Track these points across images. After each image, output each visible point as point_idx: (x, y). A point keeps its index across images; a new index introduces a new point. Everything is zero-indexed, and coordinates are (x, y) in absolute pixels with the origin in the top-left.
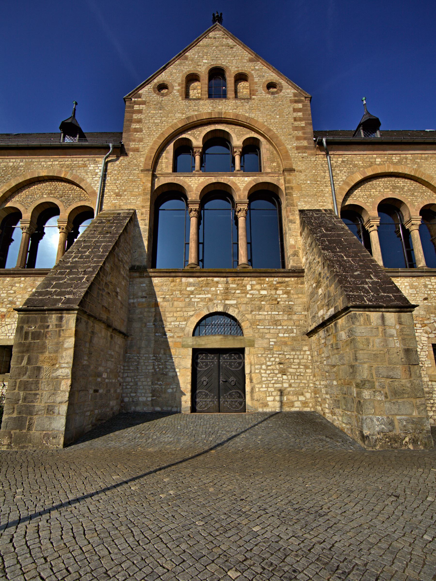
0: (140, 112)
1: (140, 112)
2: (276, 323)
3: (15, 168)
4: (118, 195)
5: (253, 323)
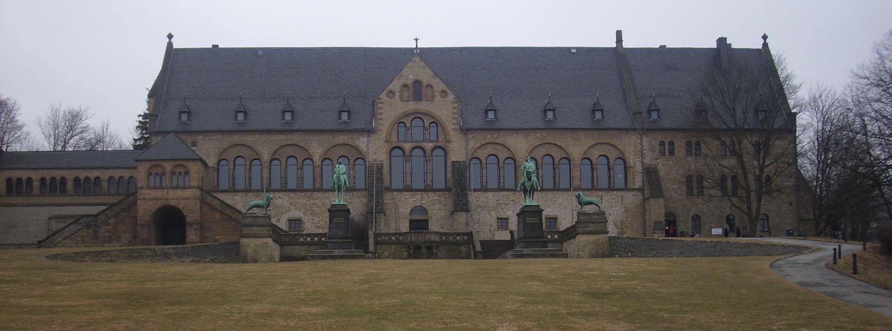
0: (381, 108)
1: (381, 108)
2: (440, 210)
4: (375, 153)
5: (432, 210)
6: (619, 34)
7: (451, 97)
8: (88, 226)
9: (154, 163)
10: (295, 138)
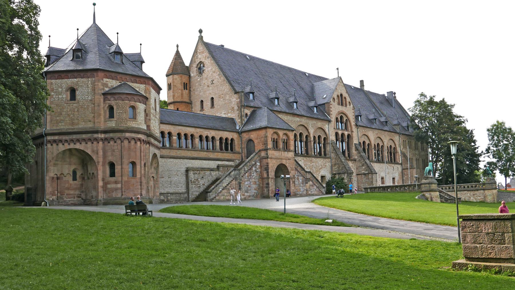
3: (315, 124)
6: (362, 82)
7: (352, 106)
8: (235, 179)
9: (275, 131)
10: (304, 121)
